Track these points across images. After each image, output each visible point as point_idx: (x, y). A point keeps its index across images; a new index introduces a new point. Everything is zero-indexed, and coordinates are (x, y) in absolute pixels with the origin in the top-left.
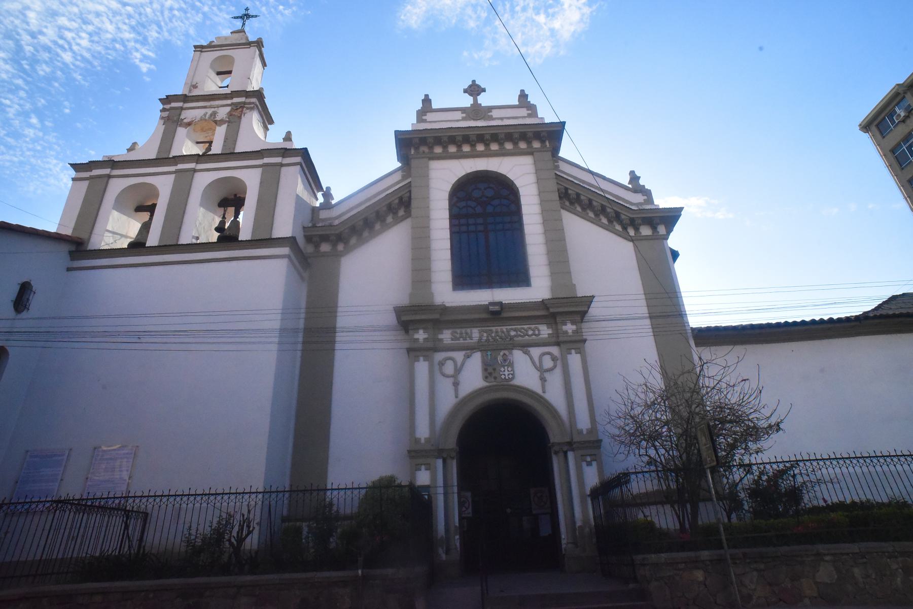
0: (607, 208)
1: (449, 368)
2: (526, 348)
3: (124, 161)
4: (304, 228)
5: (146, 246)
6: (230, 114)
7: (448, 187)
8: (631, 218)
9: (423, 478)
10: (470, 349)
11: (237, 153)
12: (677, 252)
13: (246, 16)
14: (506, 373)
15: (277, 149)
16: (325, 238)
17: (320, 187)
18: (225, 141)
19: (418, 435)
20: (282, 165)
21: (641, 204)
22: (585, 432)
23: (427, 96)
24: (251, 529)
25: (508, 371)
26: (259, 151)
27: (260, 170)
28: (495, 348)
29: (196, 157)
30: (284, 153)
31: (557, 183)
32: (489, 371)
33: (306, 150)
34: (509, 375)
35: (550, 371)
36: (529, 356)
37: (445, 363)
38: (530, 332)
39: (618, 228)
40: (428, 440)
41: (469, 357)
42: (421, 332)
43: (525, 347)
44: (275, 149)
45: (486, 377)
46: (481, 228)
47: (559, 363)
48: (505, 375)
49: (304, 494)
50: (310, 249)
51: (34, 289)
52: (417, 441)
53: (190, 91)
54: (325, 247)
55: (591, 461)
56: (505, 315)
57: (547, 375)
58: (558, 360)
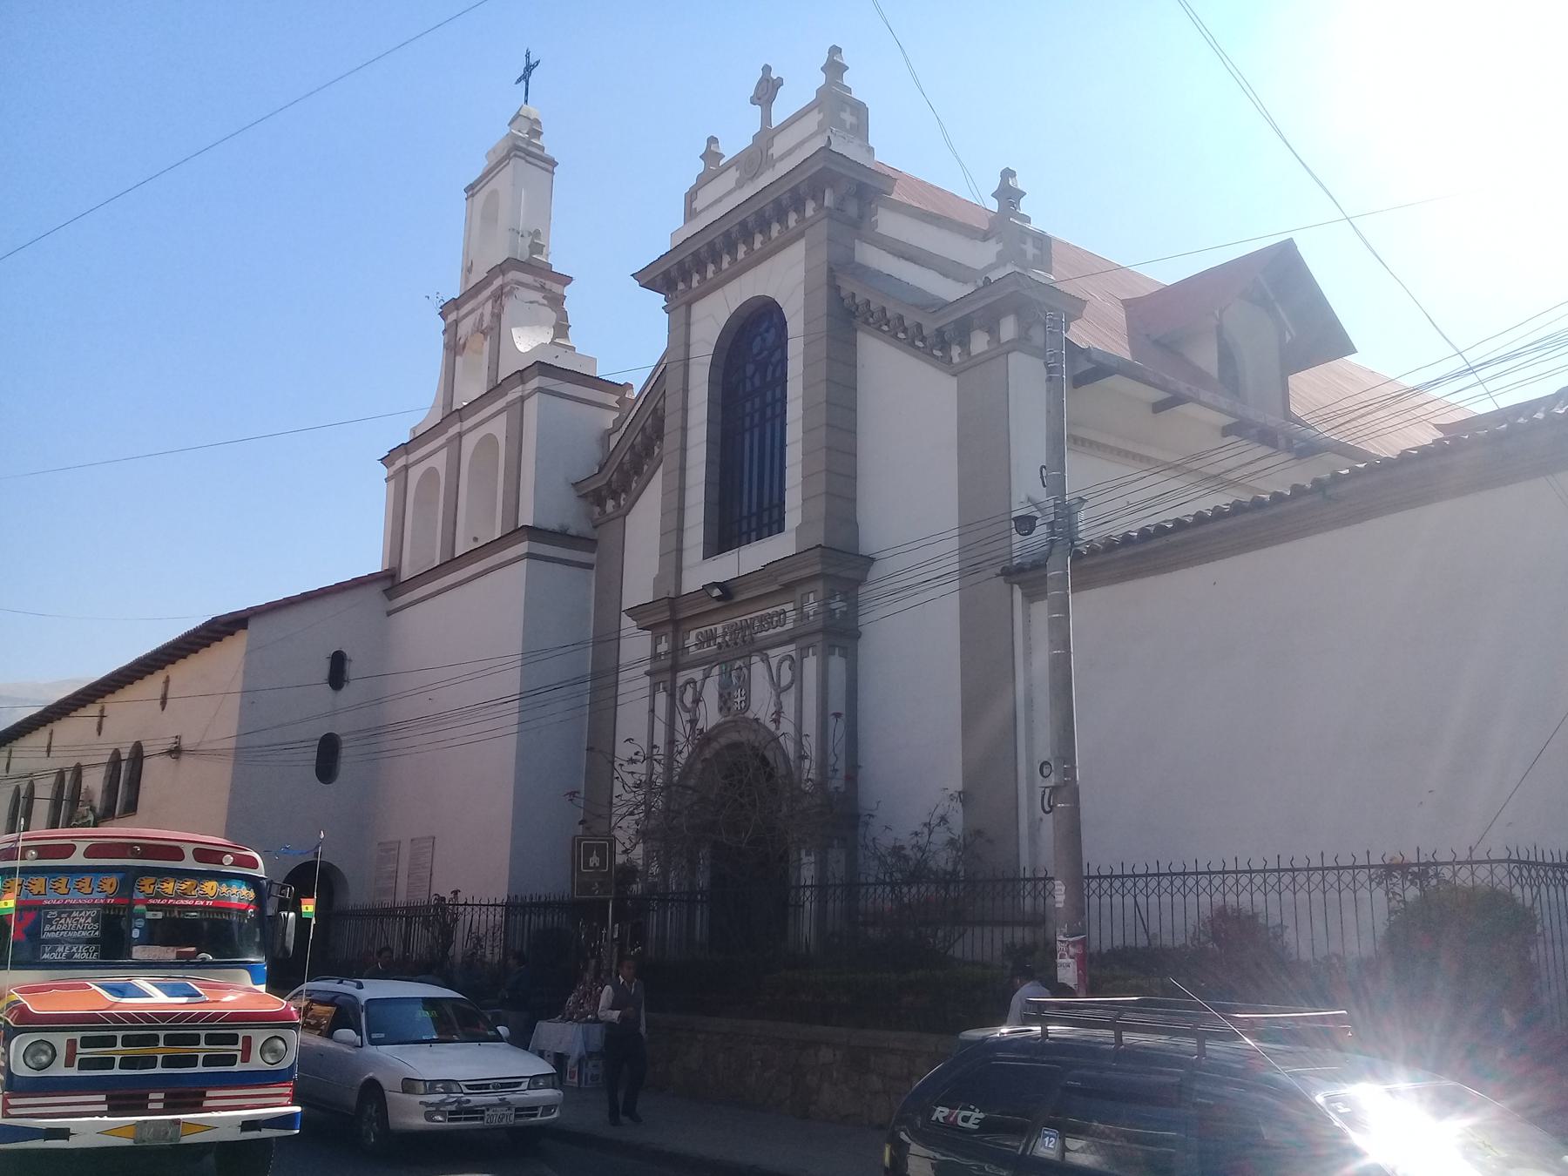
6: (493, 314)
8: (937, 330)
13: (529, 69)
15: (512, 375)
20: (522, 399)
23: (713, 140)
30: (521, 378)
31: (834, 288)
34: (741, 702)
43: (762, 650)
45: (721, 709)
50: (597, 509)
51: (348, 658)
53: (467, 282)
54: (610, 504)
56: (738, 598)
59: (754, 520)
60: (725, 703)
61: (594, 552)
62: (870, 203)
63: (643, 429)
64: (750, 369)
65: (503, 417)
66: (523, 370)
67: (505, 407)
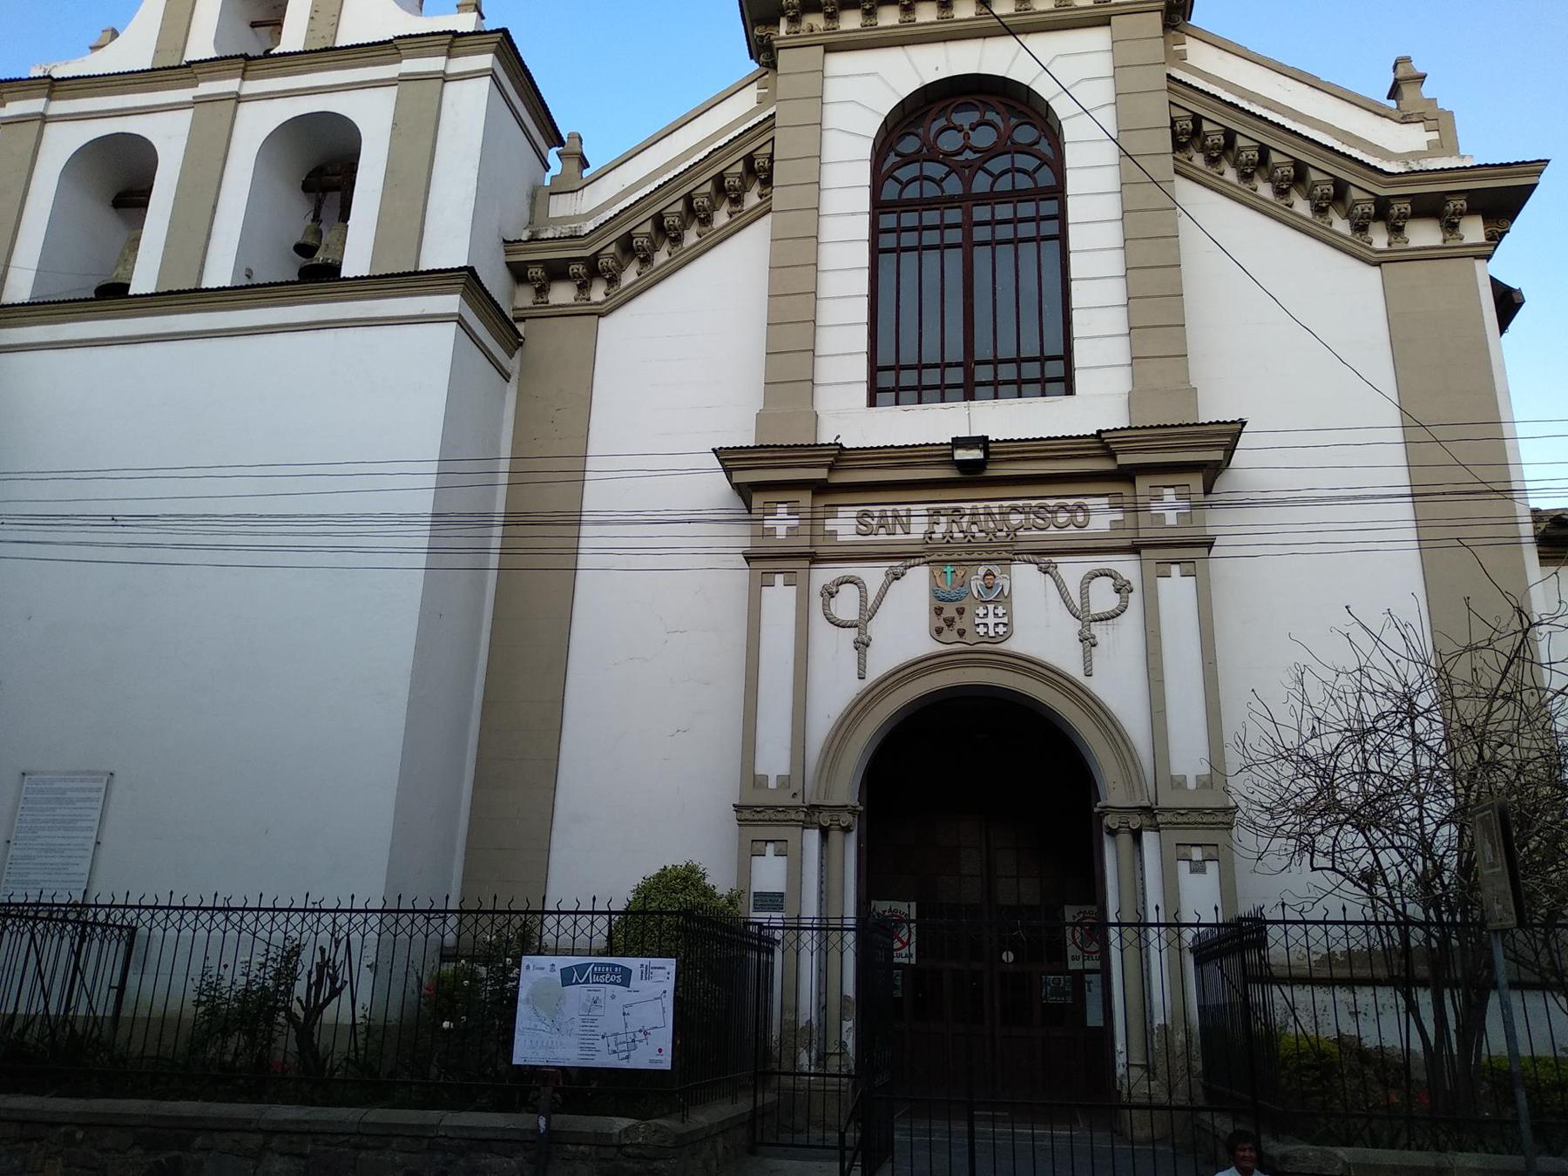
0: (1310, 169)
1: (847, 605)
2: (1046, 559)
3: (74, 78)
4: (504, 241)
5: (131, 292)
7: (873, 126)
9: (769, 873)
10: (901, 558)
11: (341, 48)
12: (1519, 292)
14: (988, 619)
15: (433, 34)
16: (557, 272)
17: (555, 138)
18: (312, 18)
19: (759, 770)
20: (445, 78)
21: (1416, 155)
22: (1191, 784)
24: (338, 985)
25: (996, 615)
26: (390, 41)
27: (393, 91)
28: (965, 556)
29: (241, 63)
30: (451, 45)
31: (1170, 102)
32: (946, 614)
33: (505, 31)
34: (996, 625)
35: (1107, 619)
36: (1054, 579)
37: (837, 592)
38: (1062, 518)
39: (1341, 226)
40: (784, 782)
41: (898, 579)
42: (782, 510)
43: (1044, 556)
44: (428, 35)
45: (939, 631)
46: (954, 236)
47: (1135, 599)
48: (986, 625)
49: (429, 919)
50: (525, 297)
52: (758, 782)
55: (1204, 861)
57: (1097, 629)
58: (1132, 591)
59: (955, 376)
60: (950, 622)
61: (511, 356)
62: (1174, 28)
63: (688, 198)
64: (934, 170)
65: (386, 99)
66: (463, 34)
67: (393, 79)
